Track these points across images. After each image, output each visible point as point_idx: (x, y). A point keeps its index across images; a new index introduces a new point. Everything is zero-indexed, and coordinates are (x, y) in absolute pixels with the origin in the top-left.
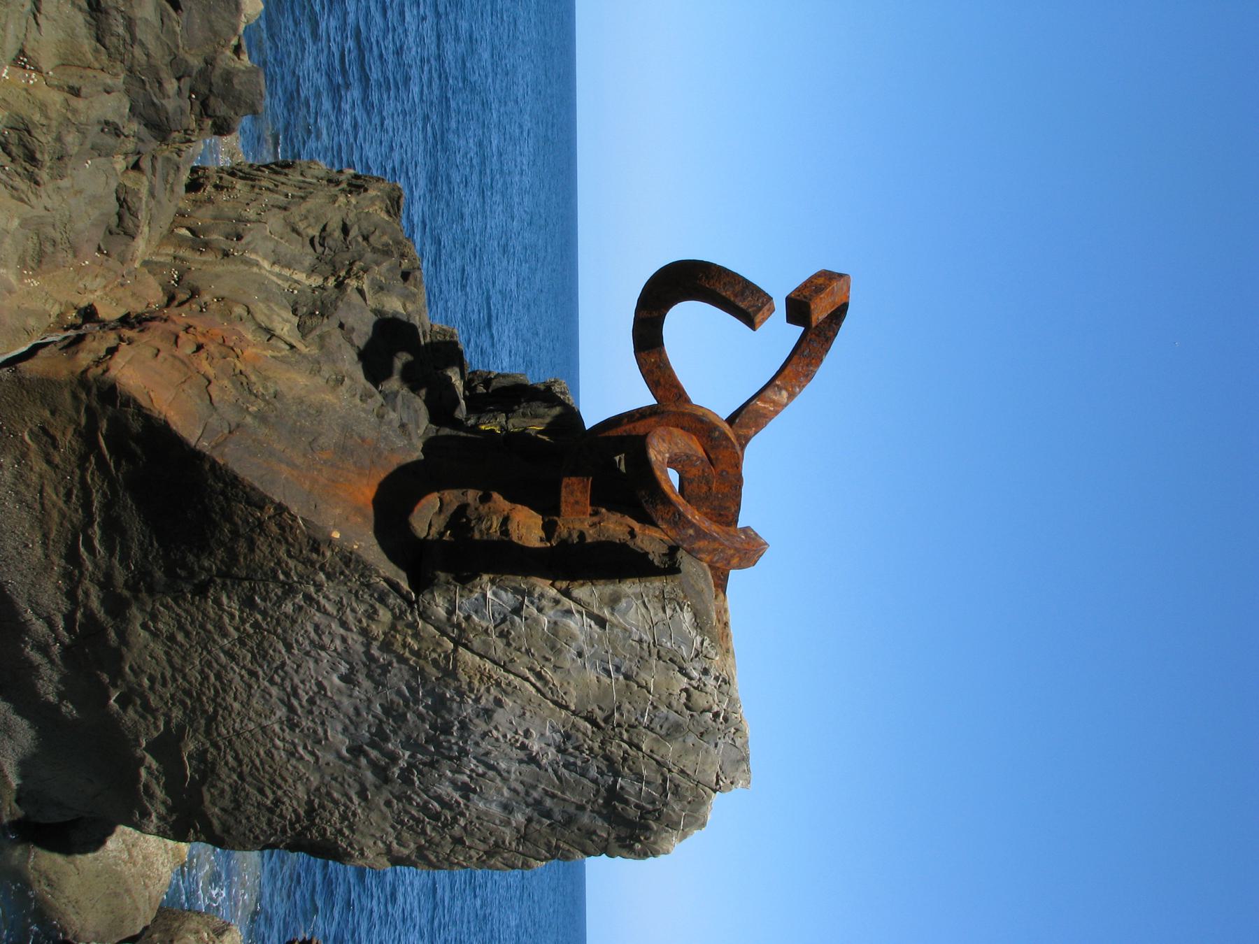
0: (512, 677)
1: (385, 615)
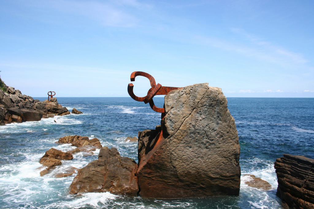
0: (184, 122)
1: (175, 140)
